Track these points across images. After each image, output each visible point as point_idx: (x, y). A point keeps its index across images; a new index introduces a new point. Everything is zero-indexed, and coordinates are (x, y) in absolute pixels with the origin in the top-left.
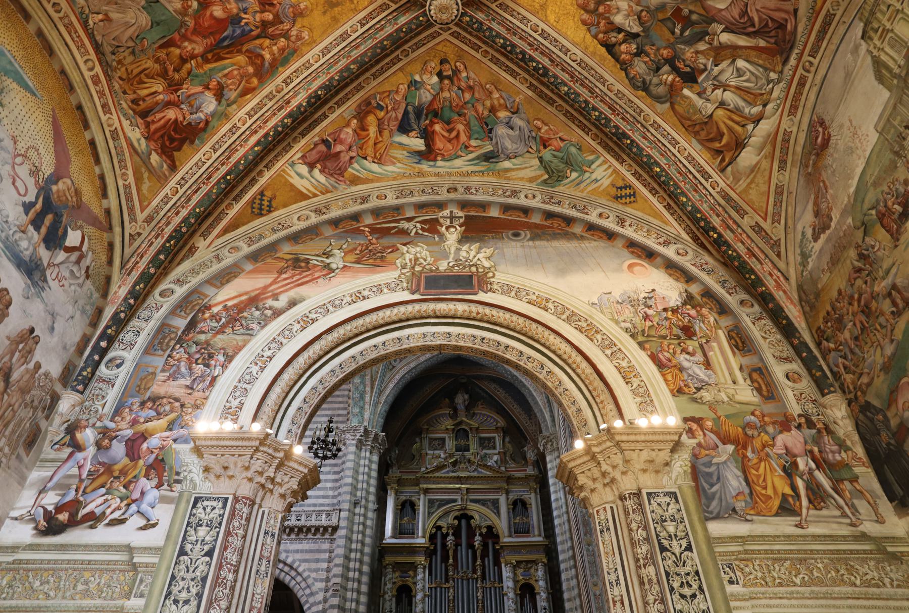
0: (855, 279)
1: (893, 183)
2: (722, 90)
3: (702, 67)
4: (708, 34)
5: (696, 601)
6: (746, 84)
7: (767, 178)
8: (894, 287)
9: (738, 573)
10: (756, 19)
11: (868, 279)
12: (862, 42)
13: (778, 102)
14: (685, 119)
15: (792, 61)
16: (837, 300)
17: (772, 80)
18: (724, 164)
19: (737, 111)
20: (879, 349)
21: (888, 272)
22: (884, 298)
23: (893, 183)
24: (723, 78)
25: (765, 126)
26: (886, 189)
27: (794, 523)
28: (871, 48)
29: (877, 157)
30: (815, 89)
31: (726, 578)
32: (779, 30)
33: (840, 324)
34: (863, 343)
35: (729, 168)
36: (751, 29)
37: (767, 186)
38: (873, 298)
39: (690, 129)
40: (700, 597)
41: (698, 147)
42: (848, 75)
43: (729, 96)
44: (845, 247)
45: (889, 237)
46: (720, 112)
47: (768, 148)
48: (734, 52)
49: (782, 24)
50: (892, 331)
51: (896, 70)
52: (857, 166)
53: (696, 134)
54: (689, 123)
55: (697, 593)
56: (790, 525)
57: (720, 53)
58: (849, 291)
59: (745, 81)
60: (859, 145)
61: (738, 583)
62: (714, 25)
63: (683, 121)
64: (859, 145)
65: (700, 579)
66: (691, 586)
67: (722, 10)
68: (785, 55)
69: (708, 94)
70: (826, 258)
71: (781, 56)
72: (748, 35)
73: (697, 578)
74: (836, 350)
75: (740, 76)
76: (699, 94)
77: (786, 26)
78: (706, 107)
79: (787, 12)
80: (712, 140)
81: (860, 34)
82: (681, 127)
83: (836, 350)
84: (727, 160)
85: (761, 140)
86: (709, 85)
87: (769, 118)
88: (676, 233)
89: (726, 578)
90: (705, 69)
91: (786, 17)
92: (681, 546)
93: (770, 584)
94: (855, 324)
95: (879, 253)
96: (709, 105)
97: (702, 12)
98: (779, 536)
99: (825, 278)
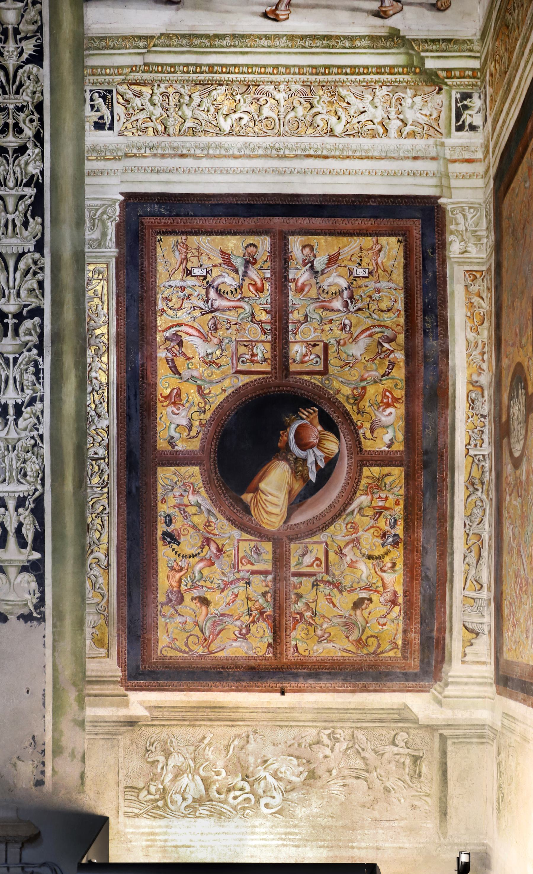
5: (23, 159)
9: (119, 109)
27: (262, 9)
31: (94, 116)
40: (32, 151)
55: (30, 145)
56: (254, 14)
61: (111, 128)
65: (41, 120)
66: (21, 131)
73: (36, 116)
89: (92, 116)
92: (21, 53)
93: (171, 131)
98: (224, 36)
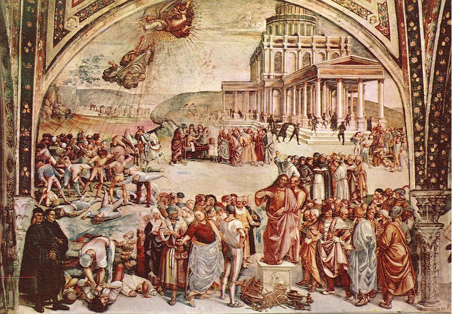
0: (118, 144)
8: (147, 184)
11: (131, 157)
12: (265, 22)
22: (133, 182)
23: (204, 130)
28: (266, 37)
33: (77, 155)
34: (88, 188)
38: (123, 172)
45: (170, 153)
58: (106, 146)
83: (55, 167)
94: (91, 170)
95: (153, 152)
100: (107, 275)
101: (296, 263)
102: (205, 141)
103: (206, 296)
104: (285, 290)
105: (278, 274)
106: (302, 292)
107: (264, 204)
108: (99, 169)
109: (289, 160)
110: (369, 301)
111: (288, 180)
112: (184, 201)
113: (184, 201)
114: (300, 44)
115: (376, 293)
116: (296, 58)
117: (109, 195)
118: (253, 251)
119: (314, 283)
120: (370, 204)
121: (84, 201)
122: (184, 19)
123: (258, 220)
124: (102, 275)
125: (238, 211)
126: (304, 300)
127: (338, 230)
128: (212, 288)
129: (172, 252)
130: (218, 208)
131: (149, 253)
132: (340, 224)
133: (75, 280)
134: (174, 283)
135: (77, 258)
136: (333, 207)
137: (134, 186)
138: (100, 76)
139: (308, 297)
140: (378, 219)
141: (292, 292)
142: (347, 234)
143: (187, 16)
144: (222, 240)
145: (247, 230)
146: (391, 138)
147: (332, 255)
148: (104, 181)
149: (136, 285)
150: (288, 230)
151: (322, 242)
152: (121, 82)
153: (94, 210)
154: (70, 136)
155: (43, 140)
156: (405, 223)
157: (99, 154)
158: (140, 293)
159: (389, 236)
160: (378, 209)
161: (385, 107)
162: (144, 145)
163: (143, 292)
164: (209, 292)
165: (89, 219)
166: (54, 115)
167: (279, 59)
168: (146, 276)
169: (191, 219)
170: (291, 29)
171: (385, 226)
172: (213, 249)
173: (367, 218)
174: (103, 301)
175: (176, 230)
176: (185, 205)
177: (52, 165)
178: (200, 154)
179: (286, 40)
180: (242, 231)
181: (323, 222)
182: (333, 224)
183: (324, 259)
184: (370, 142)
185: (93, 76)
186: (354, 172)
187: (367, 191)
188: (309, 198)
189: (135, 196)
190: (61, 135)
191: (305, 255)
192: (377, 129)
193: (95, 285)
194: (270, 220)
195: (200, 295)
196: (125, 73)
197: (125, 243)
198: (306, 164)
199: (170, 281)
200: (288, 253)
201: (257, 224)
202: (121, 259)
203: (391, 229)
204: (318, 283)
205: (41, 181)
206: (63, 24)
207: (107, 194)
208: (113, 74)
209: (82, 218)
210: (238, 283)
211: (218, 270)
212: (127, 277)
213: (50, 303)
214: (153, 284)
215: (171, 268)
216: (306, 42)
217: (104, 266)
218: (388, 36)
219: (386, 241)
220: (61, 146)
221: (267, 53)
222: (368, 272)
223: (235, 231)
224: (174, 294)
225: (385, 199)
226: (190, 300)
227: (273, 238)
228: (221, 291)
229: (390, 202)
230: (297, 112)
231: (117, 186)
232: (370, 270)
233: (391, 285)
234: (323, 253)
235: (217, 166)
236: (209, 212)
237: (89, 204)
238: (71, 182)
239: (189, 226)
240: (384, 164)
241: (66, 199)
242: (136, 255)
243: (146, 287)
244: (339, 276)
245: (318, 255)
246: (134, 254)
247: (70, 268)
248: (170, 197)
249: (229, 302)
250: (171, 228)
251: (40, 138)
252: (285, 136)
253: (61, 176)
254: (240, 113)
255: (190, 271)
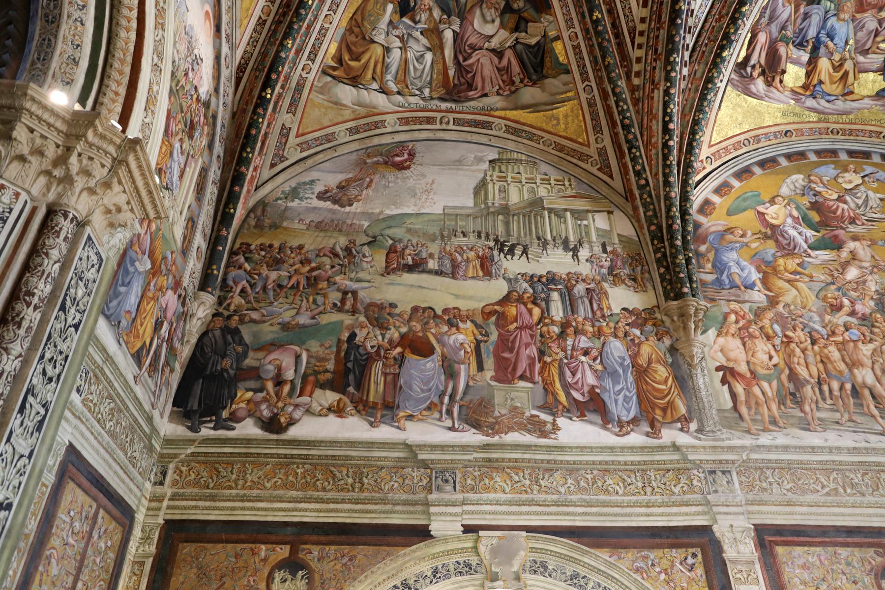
0: (325, 255)
1: (422, 245)
2: (401, 45)
3: (418, 18)
4: (449, 17)
6: (411, 68)
7: (336, 121)
8: (354, 293)
10: (471, 61)
11: (338, 267)
12: (487, 163)
13: (406, 105)
14: (362, 13)
15: (444, 106)
16: (291, 248)
17: (422, 92)
18: (331, 72)
19: (386, 68)
20: (294, 312)
21: (359, 280)
22: (338, 290)
23: (422, 245)
24: (412, 43)
25: (381, 100)
26: (414, 242)
28: (489, 173)
29: (428, 221)
30: (429, 135)
32: (466, 86)
33: (276, 263)
34: (283, 294)
35: (329, 79)
36: (461, 59)
37: (329, 124)
38: (328, 280)
39: (353, 22)
41: (338, 37)
42: (459, 163)
43: (396, 54)
44: (340, 230)
45: (384, 265)
46: (379, 50)
47: (362, 111)
48: (437, 47)
49: (472, 86)
50: (321, 313)
51: (490, 202)
52: (408, 207)
53: (349, 30)
54: (359, 20)
57: (434, 33)
58: (311, 256)
59: (414, 66)
60: (423, 200)
62: (458, 21)
63: (359, 12)
64: (423, 200)
67: (473, 25)
68: (447, 97)
69: (393, 32)
70: (317, 218)
71: (447, 93)
72: (456, 57)
74: (249, 273)
75: (417, 60)
76: (391, 22)
77: (471, 90)
78: (380, 34)
79: (483, 87)
80: (349, 50)
81: (491, 158)
82: (353, 11)
83: (249, 273)
84: (335, 73)
85: (368, 101)
86: (401, 30)
87: (389, 102)
88: (238, 42)
90: (416, 23)
91: (479, 88)
94: (290, 278)
95: (364, 264)
96: (383, 36)
97: (468, 8)
99: (296, 225)
100: (293, 389)
101: (534, 383)
102: (424, 255)
103: (420, 417)
104: (523, 413)
105: (513, 394)
106: (544, 417)
107: (494, 319)
108: (300, 277)
109: (520, 276)
110: (632, 430)
111: (519, 296)
112: (397, 311)
113: (397, 311)
114: (524, 181)
115: (639, 421)
116: (521, 191)
117: (308, 301)
118: (481, 368)
119: (560, 407)
120: (617, 323)
121: (276, 308)
122: (406, 156)
123: (487, 335)
124: (286, 388)
125: (460, 324)
126: (549, 427)
127: (582, 348)
128: (429, 408)
129: (380, 364)
130: (438, 321)
131: (350, 365)
132: (584, 342)
133: (249, 394)
134: (380, 402)
135: (257, 369)
136: (574, 324)
137: (339, 295)
138: (314, 196)
139: (554, 423)
140: (629, 338)
141: (532, 416)
142: (594, 353)
143: (410, 154)
144: (443, 355)
145: (472, 345)
146: (630, 261)
147: (579, 375)
148: (304, 288)
149: (330, 402)
150: (523, 347)
151: (565, 361)
152: (335, 202)
153: (287, 316)
154: (271, 246)
155: (240, 248)
156: (660, 343)
157: (301, 262)
158: (334, 412)
159: (646, 356)
160: (627, 328)
161: (618, 235)
162: (355, 257)
163: (338, 411)
164: (425, 413)
165: (279, 326)
166: (256, 227)
167: (504, 193)
168: (343, 391)
169: (404, 330)
170: (513, 169)
171: (639, 345)
172: (431, 364)
173: (616, 336)
174: (283, 420)
175: (386, 341)
176: (399, 315)
177: (245, 271)
178: (417, 266)
179: (509, 177)
180: (466, 345)
181: (565, 340)
182: (577, 342)
183: (570, 380)
184: (607, 264)
185: (307, 196)
186: (594, 290)
187: (611, 310)
188: (546, 315)
189: (339, 304)
190: (261, 244)
191: (546, 374)
192: (614, 252)
193: (276, 400)
194: (500, 335)
195: (411, 416)
196: (340, 195)
197: (321, 353)
198: (539, 281)
199: (375, 397)
200: (525, 371)
201: (485, 339)
202: (314, 371)
203: (646, 350)
204: (564, 407)
205: (227, 286)
206: (283, 150)
207: (305, 301)
208: (328, 194)
209: (272, 325)
210: (462, 403)
211: (437, 387)
212: (318, 392)
213: (211, 421)
214: (351, 402)
215: (377, 384)
216: (530, 179)
217: (291, 378)
218: (611, 177)
219: (642, 361)
220: (259, 254)
221: (490, 186)
222: (625, 396)
223: (458, 345)
224: (379, 415)
225: (633, 318)
226: (399, 422)
227: (506, 355)
228: (441, 412)
229: (640, 321)
230: (525, 234)
231: (318, 294)
232: (628, 394)
233: (658, 411)
234: (568, 373)
235: (438, 279)
236: (427, 323)
237: (281, 310)
238: (264, 288)
239: (403, 337)
240: (626, 285)
241: (255, 305)
242: (332, 367)
243: (341, 405)
244: (591, 399)
245: (562, 375)
246: (330, 366)
247: (245, 380)
248: (381, 307)
249: (450, 425)
250: (380, 338)
251: (237, 246)
252: (513, 255)
253: (253, 282)
254: (462, 232)
255: (401, 387)
